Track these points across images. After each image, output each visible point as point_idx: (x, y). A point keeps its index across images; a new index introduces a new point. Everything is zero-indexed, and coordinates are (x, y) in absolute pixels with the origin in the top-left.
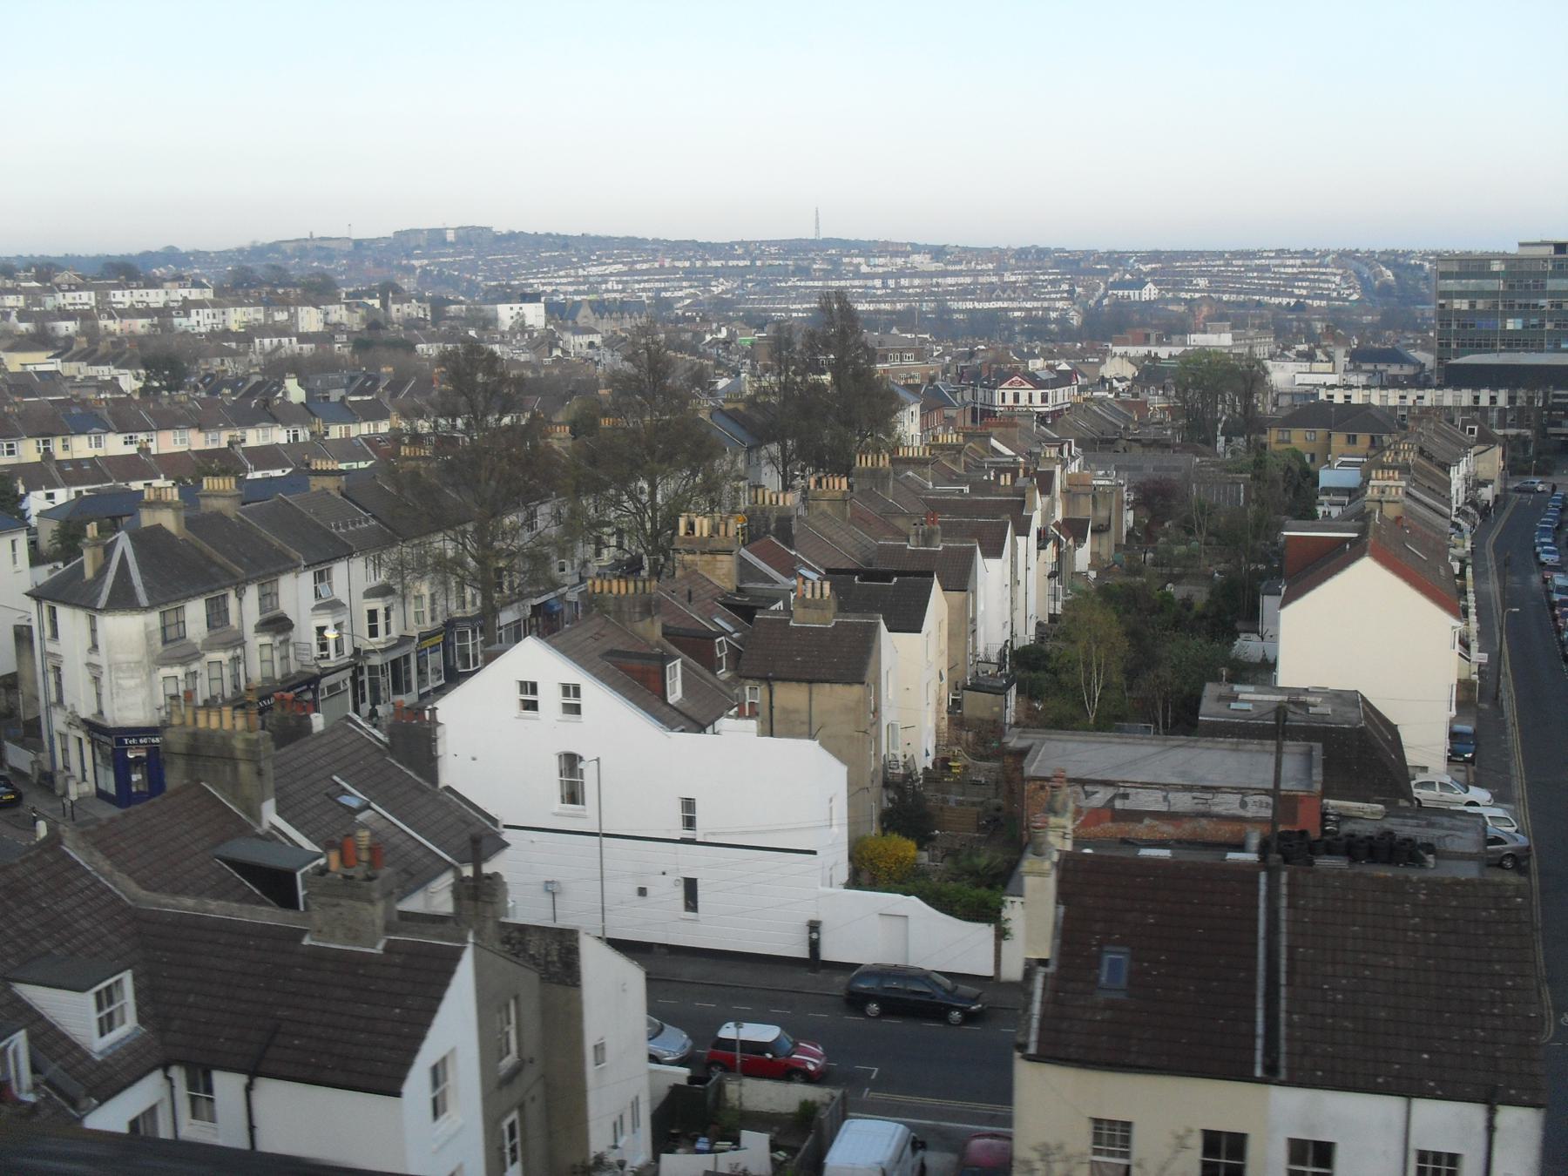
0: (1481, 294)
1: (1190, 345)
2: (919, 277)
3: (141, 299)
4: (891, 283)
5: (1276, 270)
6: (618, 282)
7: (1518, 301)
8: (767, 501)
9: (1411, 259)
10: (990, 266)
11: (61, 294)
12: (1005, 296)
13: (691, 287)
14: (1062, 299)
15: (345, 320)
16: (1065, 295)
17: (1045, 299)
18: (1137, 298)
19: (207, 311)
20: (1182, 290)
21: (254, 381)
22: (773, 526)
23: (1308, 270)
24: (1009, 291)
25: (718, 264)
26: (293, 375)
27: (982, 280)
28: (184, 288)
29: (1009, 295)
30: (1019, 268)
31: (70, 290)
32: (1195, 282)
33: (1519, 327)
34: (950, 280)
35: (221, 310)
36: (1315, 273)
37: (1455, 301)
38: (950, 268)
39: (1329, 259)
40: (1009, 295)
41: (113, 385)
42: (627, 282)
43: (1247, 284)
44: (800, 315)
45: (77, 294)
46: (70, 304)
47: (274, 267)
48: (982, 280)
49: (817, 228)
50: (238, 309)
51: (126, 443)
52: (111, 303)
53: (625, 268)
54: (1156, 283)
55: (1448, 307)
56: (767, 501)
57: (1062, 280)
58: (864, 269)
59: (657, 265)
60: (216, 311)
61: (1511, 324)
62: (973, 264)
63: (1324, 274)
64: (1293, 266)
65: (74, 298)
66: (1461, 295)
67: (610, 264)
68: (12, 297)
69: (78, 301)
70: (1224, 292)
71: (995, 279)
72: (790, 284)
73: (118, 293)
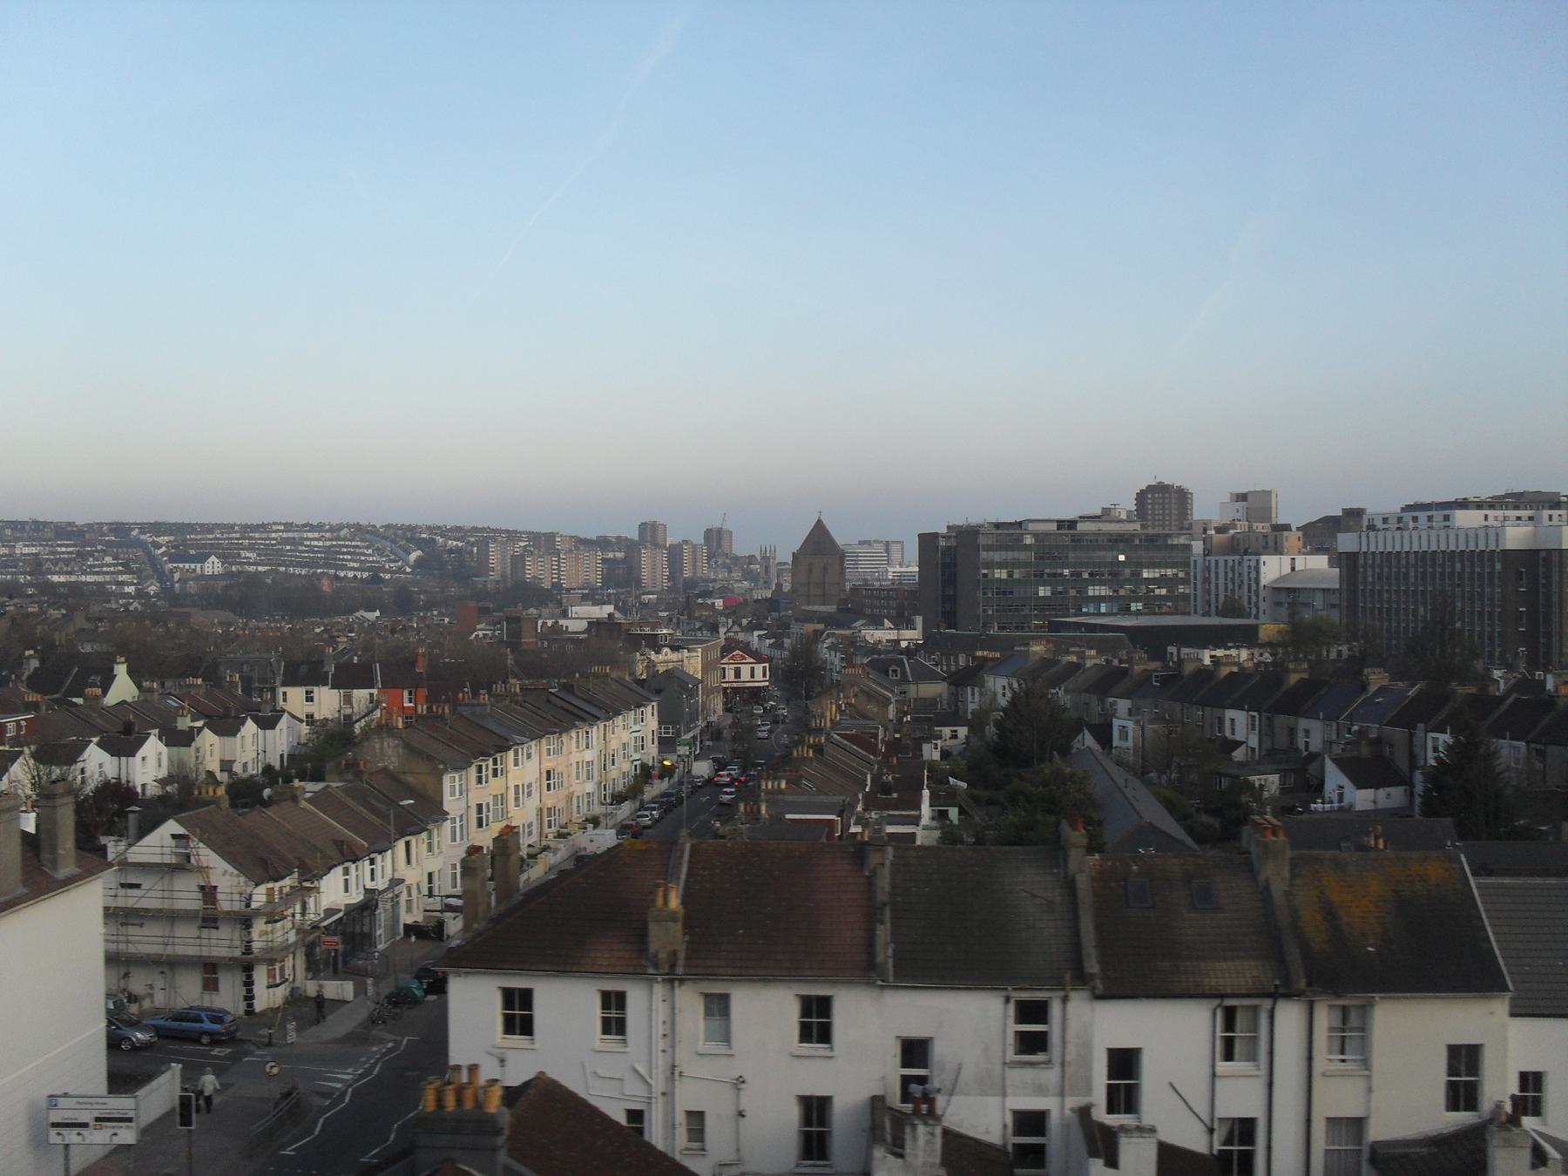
0: (1016, 564)
7: (1047, 571)
9: (420, 533)
12: (57, 569)
16: (120, 568)
21: (32, 670)
23: (342, 543)
24: (61, 564)
26: (123, 659)
29: (61, 568)
33: (1049, 594)
36: (347, 546)
37: (996, 571)
39: (344, 532)
40: (61, 568)
55: (990, 577)
61: (1043, 592)
63: (357, 547)
66: (1001, 566)
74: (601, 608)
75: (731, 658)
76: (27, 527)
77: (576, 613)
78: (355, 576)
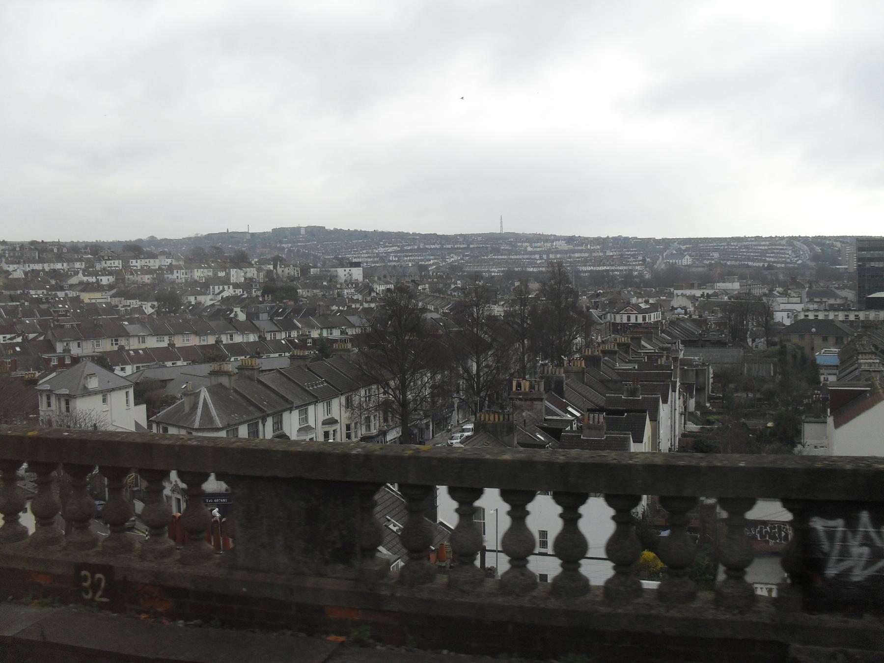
1: (717, 289)
2: (560, 253)
3: (146, 264)
4: (545, 257)
5: (756, 247)
6: (395, 257)
8: (550, 372)
10: (598, 247)
11: (104, 261)
13: (435, 259)
14: (639, 265)
15: (255, 276)
16: (641, 262)
17: (630, 265)
18: (680, 263)
19: (182, 271)
20: (705, 259)
22: (553, 386)
25: (449, 246)
27: (594, 254)
28: (169, 258)
30: (614, 248)
31: (109, 259)
32: (711, 255)
34: (577, 255)
35: (190, 270)
36: (777, 249)
38: (576, 248)
41: (140, 310)
42: (400, 256)
43: (740, 255)
44: (496, 274)
45: (112, 262)
46: (109, 267)
47: (215, 248)
48: (594, 254)
49: (502, 227)
50: (199, 270)
51: (157, 341)
52: (130, 266)
53: (399, 249)
54: (690, 256)
56: (550, 372)
57: (638, 254)
58: (529, 249)
59: (416, 247)
60: (187, 271)
62: (589, 246)
63: (781, 249)
64: (764, 245)
65: (111, 264)
67: (390, 247)
68: (78, 263)
69: (113, 265)
70: (728, 260)
71: (601, 254)
72: (489, 257)
73: (134, 261)
74: (733, 284)
75: (625, 311)
76: (620, 242)
77: (719, 287)
78: (764, 265)
